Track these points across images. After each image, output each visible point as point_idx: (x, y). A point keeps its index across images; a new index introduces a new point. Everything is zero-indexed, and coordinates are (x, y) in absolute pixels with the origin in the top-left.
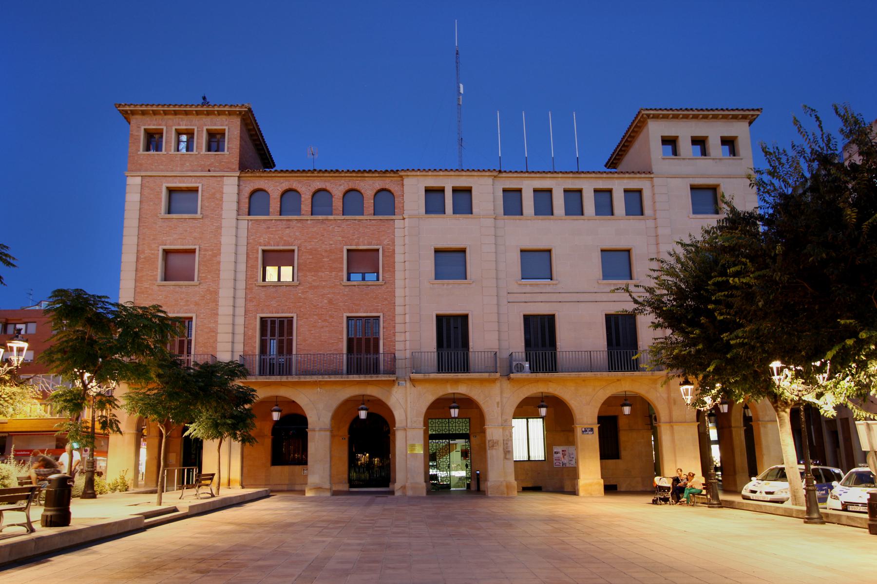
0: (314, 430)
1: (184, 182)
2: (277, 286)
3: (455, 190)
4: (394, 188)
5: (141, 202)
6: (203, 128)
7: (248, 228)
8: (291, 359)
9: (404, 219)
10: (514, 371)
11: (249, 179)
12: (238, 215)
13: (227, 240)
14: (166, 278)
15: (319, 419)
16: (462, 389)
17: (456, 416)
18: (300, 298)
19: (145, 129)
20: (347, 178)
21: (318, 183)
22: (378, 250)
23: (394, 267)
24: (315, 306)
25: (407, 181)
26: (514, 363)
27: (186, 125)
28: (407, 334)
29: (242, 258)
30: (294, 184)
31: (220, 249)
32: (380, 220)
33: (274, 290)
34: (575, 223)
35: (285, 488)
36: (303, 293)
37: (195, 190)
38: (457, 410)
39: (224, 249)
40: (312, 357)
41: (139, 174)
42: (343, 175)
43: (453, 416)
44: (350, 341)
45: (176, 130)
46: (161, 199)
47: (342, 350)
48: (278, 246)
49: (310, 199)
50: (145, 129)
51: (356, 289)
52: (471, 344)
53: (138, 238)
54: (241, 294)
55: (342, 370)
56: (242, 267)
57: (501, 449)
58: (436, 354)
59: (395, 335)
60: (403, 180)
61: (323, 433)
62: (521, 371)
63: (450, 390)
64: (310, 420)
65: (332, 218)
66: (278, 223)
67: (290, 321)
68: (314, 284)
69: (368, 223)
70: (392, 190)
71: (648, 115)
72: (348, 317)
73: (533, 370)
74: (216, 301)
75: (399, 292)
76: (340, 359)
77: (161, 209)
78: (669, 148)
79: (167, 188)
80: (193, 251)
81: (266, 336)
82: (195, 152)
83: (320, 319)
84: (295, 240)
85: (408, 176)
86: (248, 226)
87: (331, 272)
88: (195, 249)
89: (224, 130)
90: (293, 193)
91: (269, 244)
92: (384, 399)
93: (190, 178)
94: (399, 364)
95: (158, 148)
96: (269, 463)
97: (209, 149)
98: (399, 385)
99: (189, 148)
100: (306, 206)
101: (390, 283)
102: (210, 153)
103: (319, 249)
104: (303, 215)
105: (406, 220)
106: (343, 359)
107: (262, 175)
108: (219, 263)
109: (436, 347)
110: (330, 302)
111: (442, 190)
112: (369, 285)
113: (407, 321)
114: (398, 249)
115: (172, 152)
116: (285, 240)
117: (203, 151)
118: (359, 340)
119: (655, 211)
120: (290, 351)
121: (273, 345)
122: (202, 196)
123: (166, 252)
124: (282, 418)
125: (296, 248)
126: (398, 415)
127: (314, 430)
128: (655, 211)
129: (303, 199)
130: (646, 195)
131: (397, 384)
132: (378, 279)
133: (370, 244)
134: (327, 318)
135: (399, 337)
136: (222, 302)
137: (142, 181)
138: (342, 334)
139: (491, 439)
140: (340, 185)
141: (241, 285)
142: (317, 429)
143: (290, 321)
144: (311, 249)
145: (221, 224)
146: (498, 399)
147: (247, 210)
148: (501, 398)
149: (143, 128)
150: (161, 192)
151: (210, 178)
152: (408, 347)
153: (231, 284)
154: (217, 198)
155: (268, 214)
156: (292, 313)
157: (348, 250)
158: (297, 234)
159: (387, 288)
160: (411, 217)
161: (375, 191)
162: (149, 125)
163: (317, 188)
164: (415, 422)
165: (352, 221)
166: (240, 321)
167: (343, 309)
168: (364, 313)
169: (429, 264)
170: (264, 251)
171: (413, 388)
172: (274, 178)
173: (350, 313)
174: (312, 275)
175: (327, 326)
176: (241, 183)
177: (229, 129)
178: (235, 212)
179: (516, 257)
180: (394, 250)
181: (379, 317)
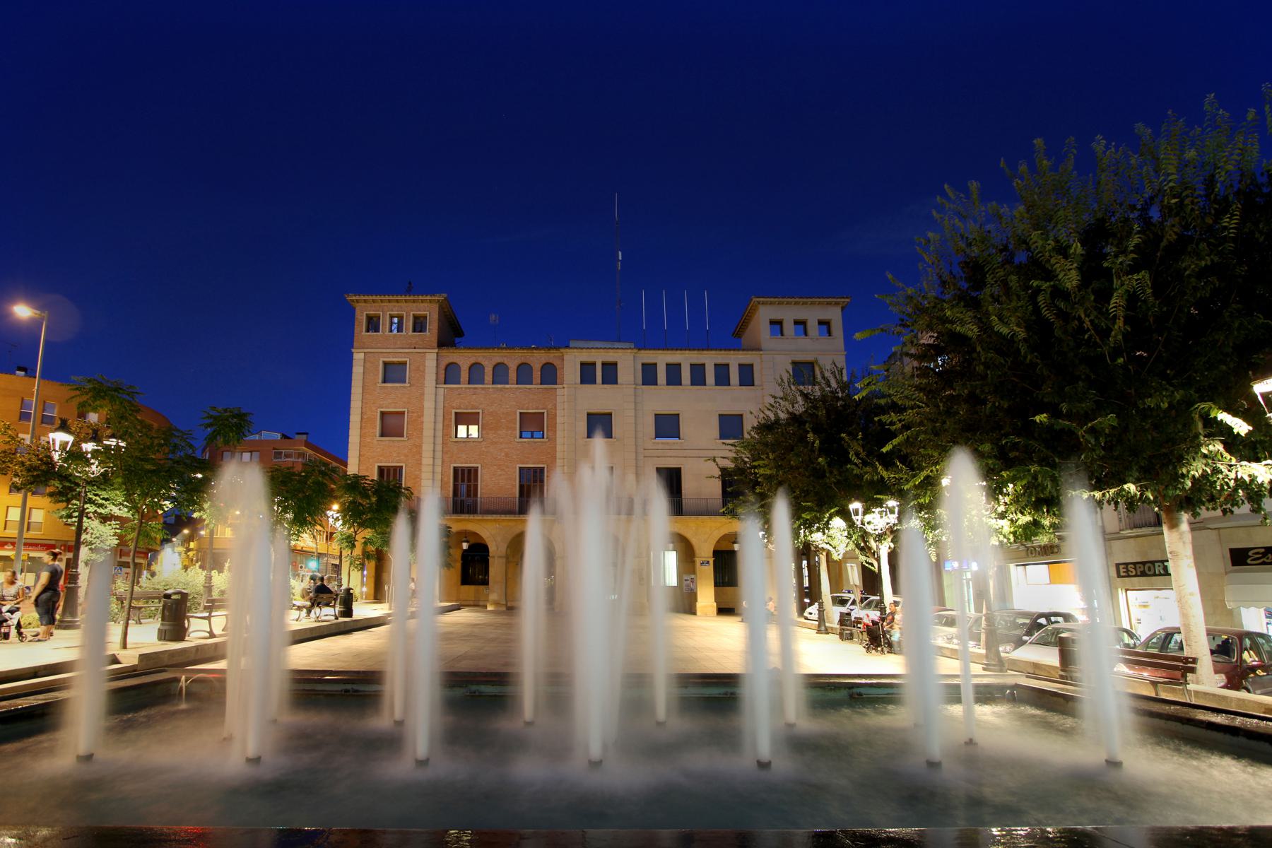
0: (493, 557)
3: (604, 364)
4: (556, 363)
12: (437, 384)
13: (428, 405)
14: (382, 435)
19: (367, 314)
22: (543, 413)
23: (556, 427)
29: (440, 419)
31: (423, 412)
33: (464, 445)
35: (472, 603)
37: (405, 363)
39: (426, 412)
44: (521, 487)
46: (379, 370)
47: (515, 494)
49: (491, 372)
54: (439, 448)
56: (440, 426)
67: (476, 470)
70: (555, 364)
71: (759, 303)
74: (420, 453)
75: (559, 448)
79: (383, 362)
80: (403, 413)
81: (458, 482)
82: (404, 333)
88: (404, 412)
90: (478, 365)
93: (400, 354)
95: (377, 330)
96: (460, 583)
97: (414, 331)
99: (400, 329)
100: (488, 377)
101: (553, 440)
108: (423, 422)
110: (507, 455)
111: (594, 364)
117: (411, 333)
120: (476, 495)
121: (463, 488)
123: (383, 414)
124: (469, 547)
125: (480, 411)
129: (486, 371)
130: (756, 369)
132: (543, 438)
143: (476, 470)
149: (365, 313)
153: (432, 440)
154: (421, 370)
155: (459, 384)
157: (521, 413)
161: (541, 365)
166: (438, 469)
170: (456, 413)
180: (556, 414)
181: (544, 468)
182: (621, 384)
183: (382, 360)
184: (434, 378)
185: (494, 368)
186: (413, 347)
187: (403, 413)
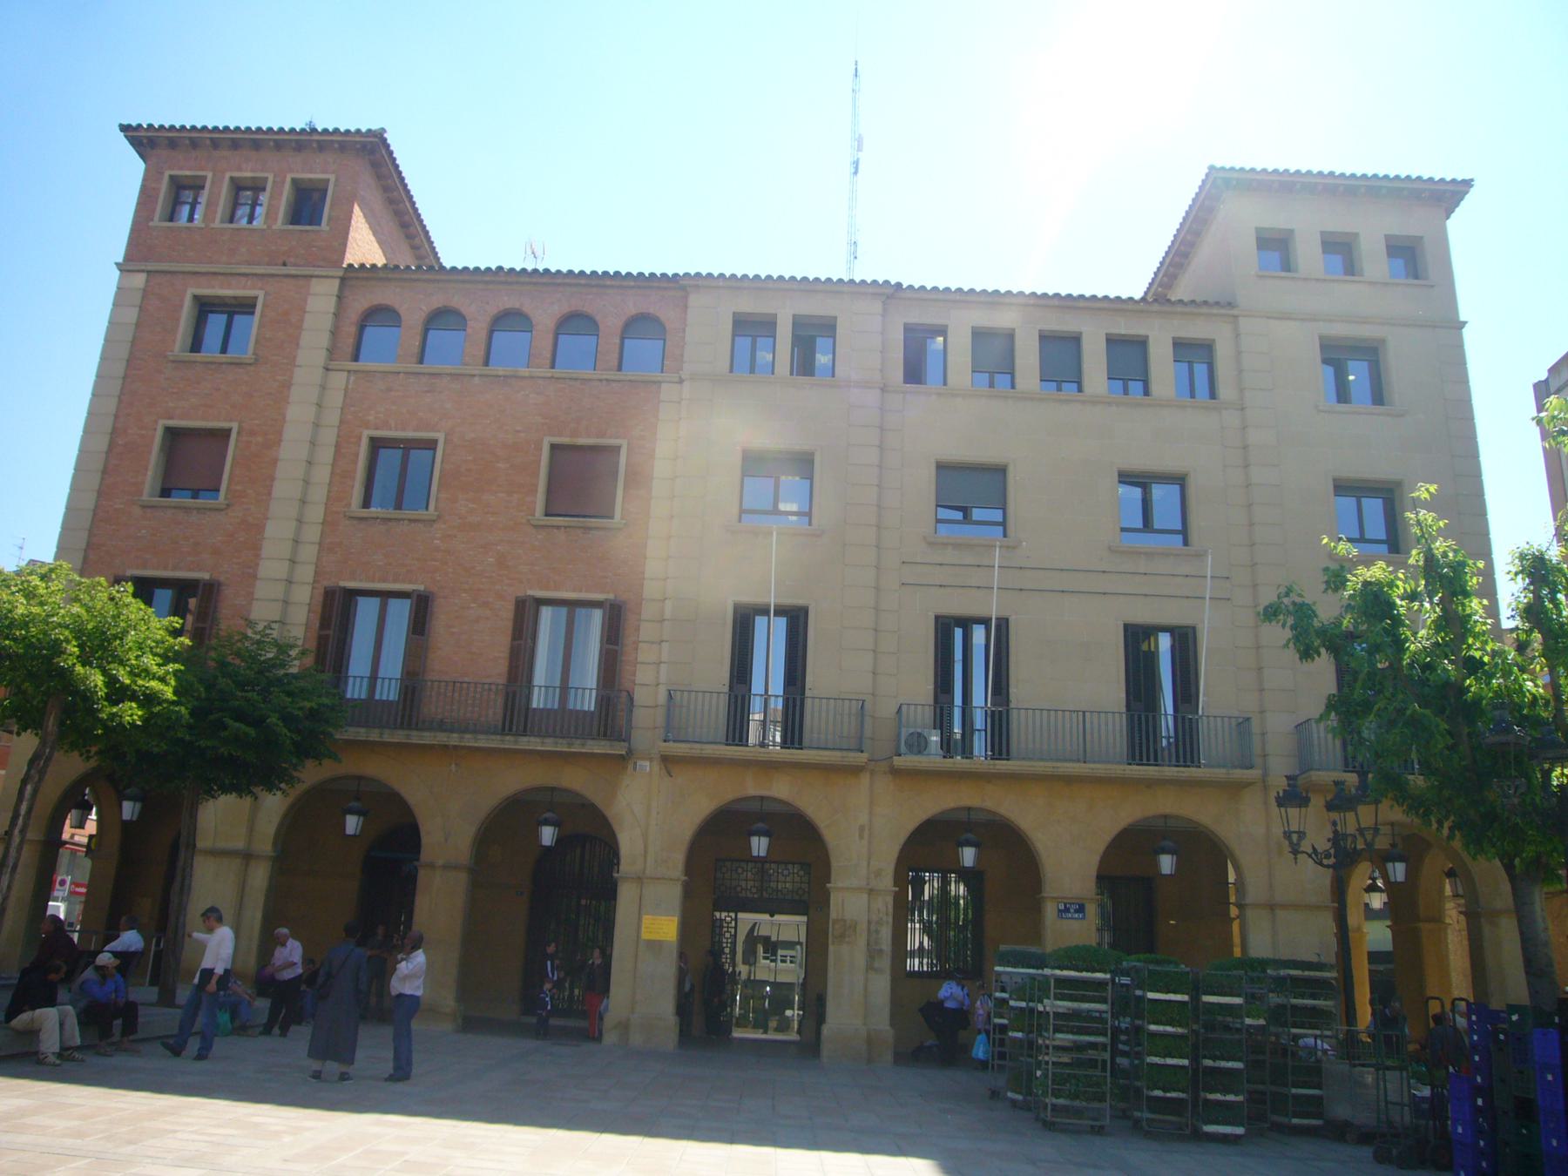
0: (432, 866)
2: (390, 520)
4: (667, 315)
5: (138, 325)
6: (285, 177)
7: (346, 389)
9: (681, 381)
10: (903, 748)
13: (298, 412)
15: (446, 840)
19: (171, 177)
25: (694, 300)
26: (904, 733)
27: (252, 171)
29: (326, 455)
30: (457, 301)
31: (280, 433)
32: (630, 381)
38: (764, 841)
39: (290, 433)
40: (450, 688)
41: (143, 268)
43: (755, 853)
45: (232, 179)
46: (178, 320)
48: (404, 429)
50: (171, 177)
52: (808, 678)
53: (120, 401)
54: (312, 533)
56: (322, 474)
57: (862, 941)
58: (724, 700)
60: (686, 298)
62: (920, 752)
64: (426, 840)
65: (527, 374)
74: (256, 548)
77: (174, 341)
78: (1274, 257)
80: (226, 433)
92: (598, 800)
93: (243, 280)
98: (635, 769)
102: (291, 227)
105: (685, 383)
107: (390, 276)
108: (275, 462)
109: (727, 682)
117: (279, 224)
119: (1242, 390)
123: (173, 434)
125: (441, 437)
126: (628, 842)
128: (1242, 390)
130: (1223, 353)
131: (630, 767)
134: (491, 600)
136: (268, 549)
141: (316, 513)
142: (440, 862)
146: (863, 819)
149: (167, 174)
152: (663, 679)
154: (289, 323)
157: (554, 447)
162: (181, 169)
163: (502, 308)
177: (337, 180)
178: (320, 357)
183: (191, 292)
184: (324, 340)
187: (226, 433)
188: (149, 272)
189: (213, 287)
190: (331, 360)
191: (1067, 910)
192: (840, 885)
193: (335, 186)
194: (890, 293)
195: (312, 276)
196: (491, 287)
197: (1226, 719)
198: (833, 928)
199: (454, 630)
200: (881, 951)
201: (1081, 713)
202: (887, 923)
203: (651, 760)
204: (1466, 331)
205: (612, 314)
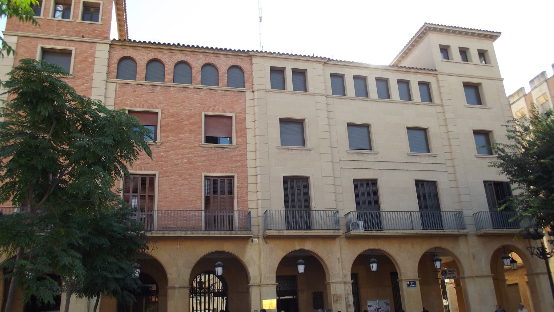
0: (174, 288)
1: (58, 45)
3: (295, 72)
7: (116, 90)
8: (152, 216)
9: (253, 92)
11: (119, 47)
12: (108, 78)
15: (179, 277)
16: (308, 246)
17: (303, 272)
18: (162, 157)
20: (205, 54)
21: (180, 56)
22: (231, 117)
23: (246, 134)
24: (175, 165)
25: (255, 60)
28: (259, 193)
30: (160, 55)
34: (384, 105)
36: (165, 152)
37: (68, 53)
38: (303, 266)
41: (16, 34)
42: (202, 51)
44: (207, 199)
48: (143, 107)
51: (213, 151)
55: (201, 227)
59: (248, 195)
60: (251, 60)
61: (182, 291)
63: (298, 246)
64: (170, 277)
65: (193, 87)
66: (144, 87)
68: (175, 144)
69: (223, 93)
72: (205, 176)
73: (366, 228)
75: (250, 156)
76: (198, 216)
82: (71, 19)
83: (180, 177)
84: (159, 104)
85: (256, 56)
86: (116, 88)
87: (190, 134)
89: (100, 4)
91: (135, 106)
94: (254, 221)
97: (83, 19)
99: (66, 14)
103: (180, 113)
104: (166, 82)
105: (255, 92)
106: (201, 216)
107: (131, 45)
109: (284, 207)
110: (190, 162)
112: (224, 148)
113: (259, 181)
114: (249, 117)
115: (50, 17)
116: (149, 104)
117: (79, 20)
118: (215, 198)
119: (442, 100)
122: (75, 58)
126: (253, 271)
127: (174, 288)
128: (442, 100)
131: (250, 241)
132: (231, 142)
133: (225, 112)
135: (252, 196)
137: (18, 40)
138: (200, 192)
139: (335, 293)
140: (199, 59)
142: (177, 286)
144: (173, 113)
145: (91, 85)
146: (339, 255)
147: (116, 74)
148: (341, 254)
150: (36, 52)
151: (84, 43)
152: (260, 206)
155: (135, 79)
156: (154, 171)
158: (160, 98)
159: (240, 151)
160: (259, 90)
161: (228, 67)
163: (179, 60)
164: (269, 278)
165: (209, 90)
167: (202, 169)
168: (220, 172)
169: (275, 131)
171: (265, 245)
172: (142, 49)
173: (207, 172)
174: (174, 137)
175: (186, 185)
176: (112, 51)
177: (103, 3)
179: (344, 131)
182: (313, 94)
184: (105, 69)
185: (174, 67)
186: (81, 35)
188: (18, 36)
189: (51, 45)
190: (108, 78)
191: (410, 284)
192: (333, 281)
193: (103, 6)
194: (326, 62)
195: (96, 43)
196: (173, 51)
197: (448, 213)
198: (333, 298)
199: (173, 189)
200: (350, 305)
201: (410, 212)
202: (351, 294)
203: (258, 238)
204: (504, 82)
205: (223, 64)
